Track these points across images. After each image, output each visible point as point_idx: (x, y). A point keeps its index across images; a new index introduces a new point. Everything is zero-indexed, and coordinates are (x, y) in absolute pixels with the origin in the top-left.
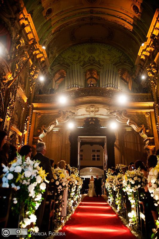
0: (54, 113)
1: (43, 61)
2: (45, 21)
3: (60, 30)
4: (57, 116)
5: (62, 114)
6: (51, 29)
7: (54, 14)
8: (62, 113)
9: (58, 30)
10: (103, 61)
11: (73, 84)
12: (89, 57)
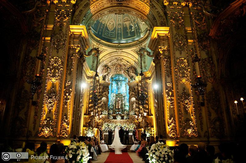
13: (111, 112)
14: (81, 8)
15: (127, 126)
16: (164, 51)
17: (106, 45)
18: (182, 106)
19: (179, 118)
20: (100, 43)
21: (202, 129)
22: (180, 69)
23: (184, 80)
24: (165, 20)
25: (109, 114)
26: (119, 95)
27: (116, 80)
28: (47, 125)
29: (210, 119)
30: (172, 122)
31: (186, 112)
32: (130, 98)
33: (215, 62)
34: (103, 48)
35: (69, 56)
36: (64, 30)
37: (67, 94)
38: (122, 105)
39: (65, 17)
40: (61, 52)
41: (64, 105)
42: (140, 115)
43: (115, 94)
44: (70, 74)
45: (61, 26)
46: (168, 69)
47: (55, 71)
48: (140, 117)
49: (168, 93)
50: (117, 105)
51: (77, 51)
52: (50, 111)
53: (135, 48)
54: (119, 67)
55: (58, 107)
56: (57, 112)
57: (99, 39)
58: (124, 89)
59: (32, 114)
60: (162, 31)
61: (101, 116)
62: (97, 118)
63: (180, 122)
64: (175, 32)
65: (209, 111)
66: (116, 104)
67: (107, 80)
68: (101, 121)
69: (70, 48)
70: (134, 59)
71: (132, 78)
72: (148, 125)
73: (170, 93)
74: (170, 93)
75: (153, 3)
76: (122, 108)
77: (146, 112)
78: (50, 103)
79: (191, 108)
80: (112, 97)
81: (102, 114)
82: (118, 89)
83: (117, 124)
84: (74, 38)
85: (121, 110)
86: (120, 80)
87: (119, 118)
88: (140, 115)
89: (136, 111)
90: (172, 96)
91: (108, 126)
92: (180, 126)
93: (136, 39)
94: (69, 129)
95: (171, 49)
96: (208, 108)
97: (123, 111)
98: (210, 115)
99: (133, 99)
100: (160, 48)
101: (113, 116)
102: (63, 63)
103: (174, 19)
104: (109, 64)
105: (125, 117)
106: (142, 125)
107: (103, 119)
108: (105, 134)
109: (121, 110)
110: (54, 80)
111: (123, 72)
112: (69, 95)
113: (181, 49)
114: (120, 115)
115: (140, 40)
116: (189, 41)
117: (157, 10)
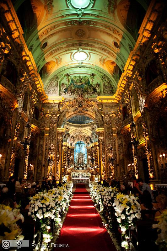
13: (76, 165)
14: (61, 118)
15: (85, 174)
16: (101, 139)
17: (72, 125)
18: (108, 166)
19: (107, 172)
20: (69, 125)
21: (117, 176)
22: (108, 149)
23: (109, 154)
24: (103, 123)
25: (74, 166)
26: (80, 154)
27: (78, 143)
28: (51, 175)
29: (120, 172)
30: (104, 173)
31: (110, 169)
32: (87, 156)
33: (124, 146)
34: (71, 127)
35: (58, 143)
36: (55, 131)
37: (58, 161)
38: (82, 160)
39: (55, 124)
40: (54, 142)
41: (56, 166)
42: (93, 167)
43: (78, 154)
44: (58, 152)
45: (53, 128)
46: (103, 149)
47: (52, 151)
48: (93, 169)
49: (103, 160)
50: (79, 161)
51: (61, 140)
52: (51, 169)
53: (90, 127)
54: (80, 137)
55: (54, 167)
56: (54, 169)
57: (68, 123)
58: (84, 150)
59: (43, 170)
60: (101, 129)
61: (70, 168)
62: (68, 169)
63: (107, 173)
64: (107, 130)
65: (120, 168)
66: (78, 160)
67: (73, 145)
68: (70, 171)
69: (57, 139)
70: (90, 133)
71: (88, 144)
72: (97, 173)
73: (104, 160)
74: (104, 160)
75: (97, 114)
76: (82, 162)
77: (96, 166)
78: (51, 165)
79: (112, 167)
80: (76, 155)
81: (70, 167)
82: (80, 149)
83: (80, 173)
84: (59, 134)
85: (82, 164)
86: (81, 143)
87: (81, 169)
88: (93, 167)
89: (91, 165)
90: (105, 161)
91: (75, 174)
92: (107, 175)
93: (91, 122)
94: (59, 177)
95: (105, 138)
96: (120, 167)
97: (83, 164)
98: (120, 170)
99: (89, 157)
100: (100, 138)
101: (77, 168)
102: (55, 147)
103: (106, 124)
104: (74, 136)
105: (84, 168)
106: (94, 173)
107: (71, 169)
108: (73, 178)
109: (82, 164)
110: (52, 155)
111: (83, 140)
112: (59, 161)
113: (109, 139)
114: (81, 167)
115: (93, 123)
116: (113, 134)
117: (99, 118)
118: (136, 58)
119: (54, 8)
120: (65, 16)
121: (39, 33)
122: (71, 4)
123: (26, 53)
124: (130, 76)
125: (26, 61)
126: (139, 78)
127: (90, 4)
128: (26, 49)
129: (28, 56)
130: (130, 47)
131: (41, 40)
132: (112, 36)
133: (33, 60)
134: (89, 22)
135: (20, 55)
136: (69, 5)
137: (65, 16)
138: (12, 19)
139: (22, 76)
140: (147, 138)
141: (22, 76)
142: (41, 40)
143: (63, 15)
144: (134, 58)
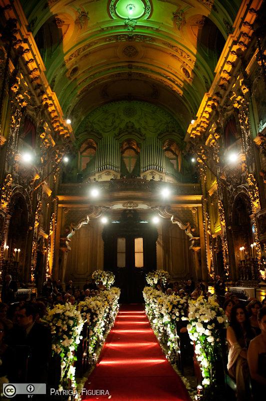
0: (84, 208)
1: (68, 137)
2: (69, 82)
3: (87, 90)
4: (89, 212)
5: (93, 208)
6: (76, 91)
7: (80, 72)
8: (94, 208)
9: (85, 90)
10: (145, 129)
11: (106, 164)
12: (127, 123)
118: (213, 104)
119: (89, 21)
120: (105, 29)
121: (66, 58)
122: (116, 13)
123: (48, 95)
124: (205, 126)
125: (47, 106)
126: (216, 136)
127: (144, 14)
128: (49, 91)
129: (50, 98)
130: (206, 82)
131: (68, 66)
132: (179, 59)
133: (56, 102)
134: (145, 37)
135: (39, 100)
136: (112, 15)
137: (105, 29)
138: (28, 48)
139: (42, 130)
140: (223, 223)
141: (42, 130)
142: (68, 66)
143: (102, 27)
144: (210, 103)
